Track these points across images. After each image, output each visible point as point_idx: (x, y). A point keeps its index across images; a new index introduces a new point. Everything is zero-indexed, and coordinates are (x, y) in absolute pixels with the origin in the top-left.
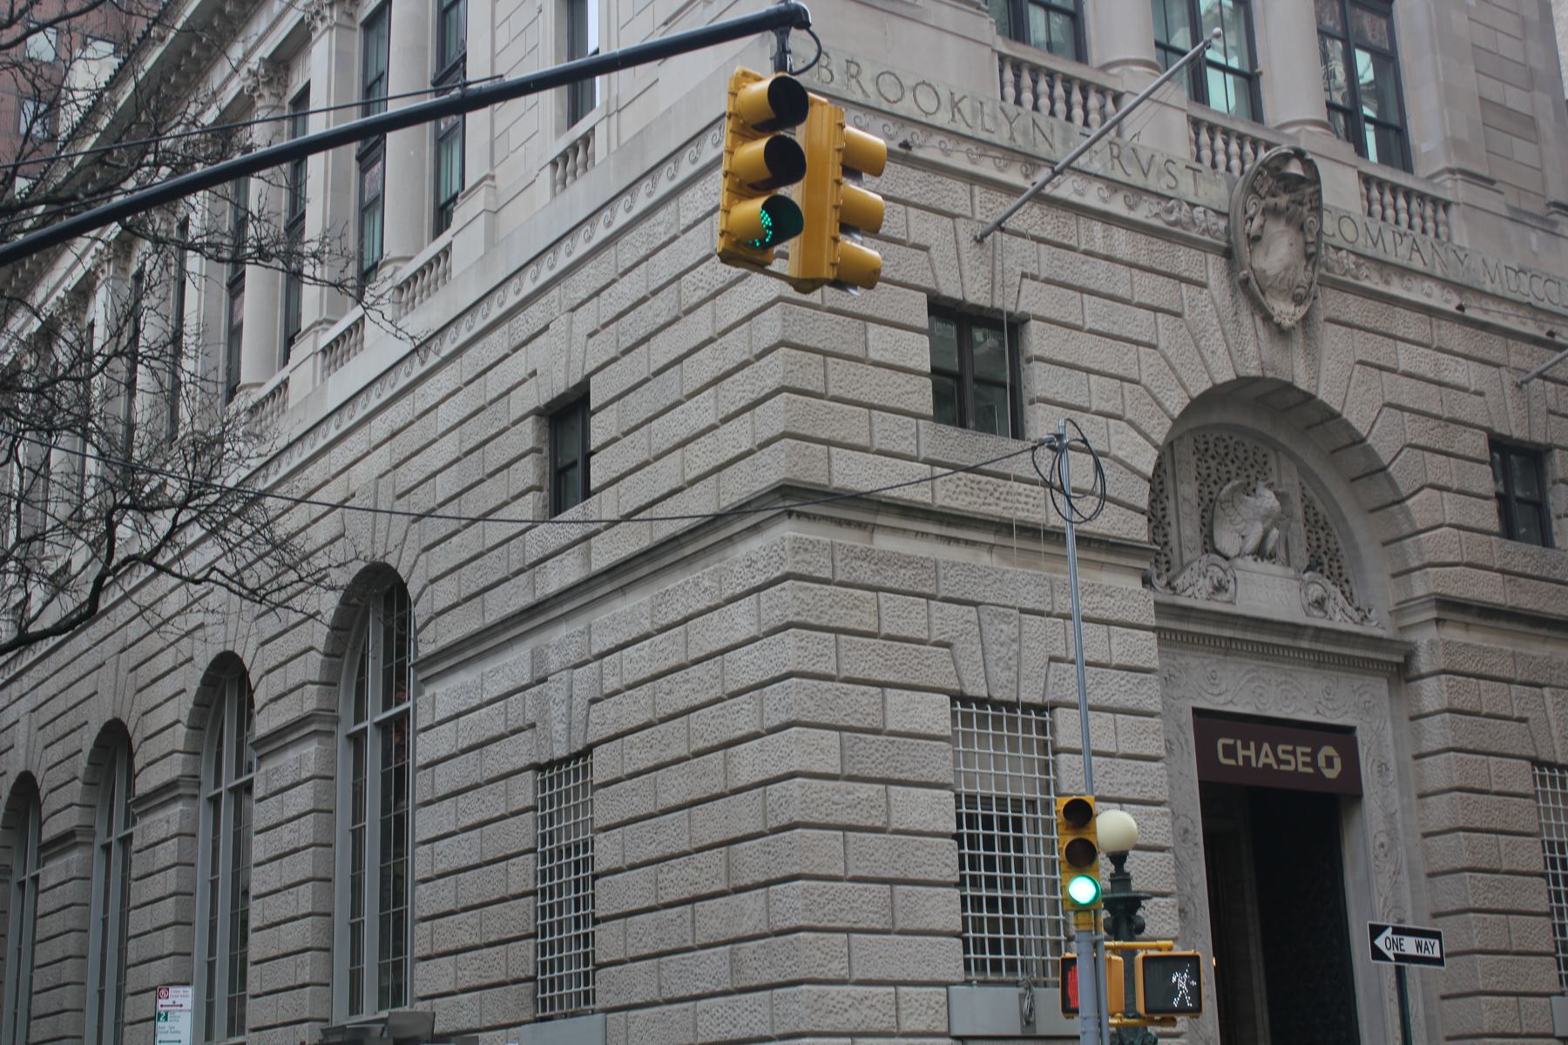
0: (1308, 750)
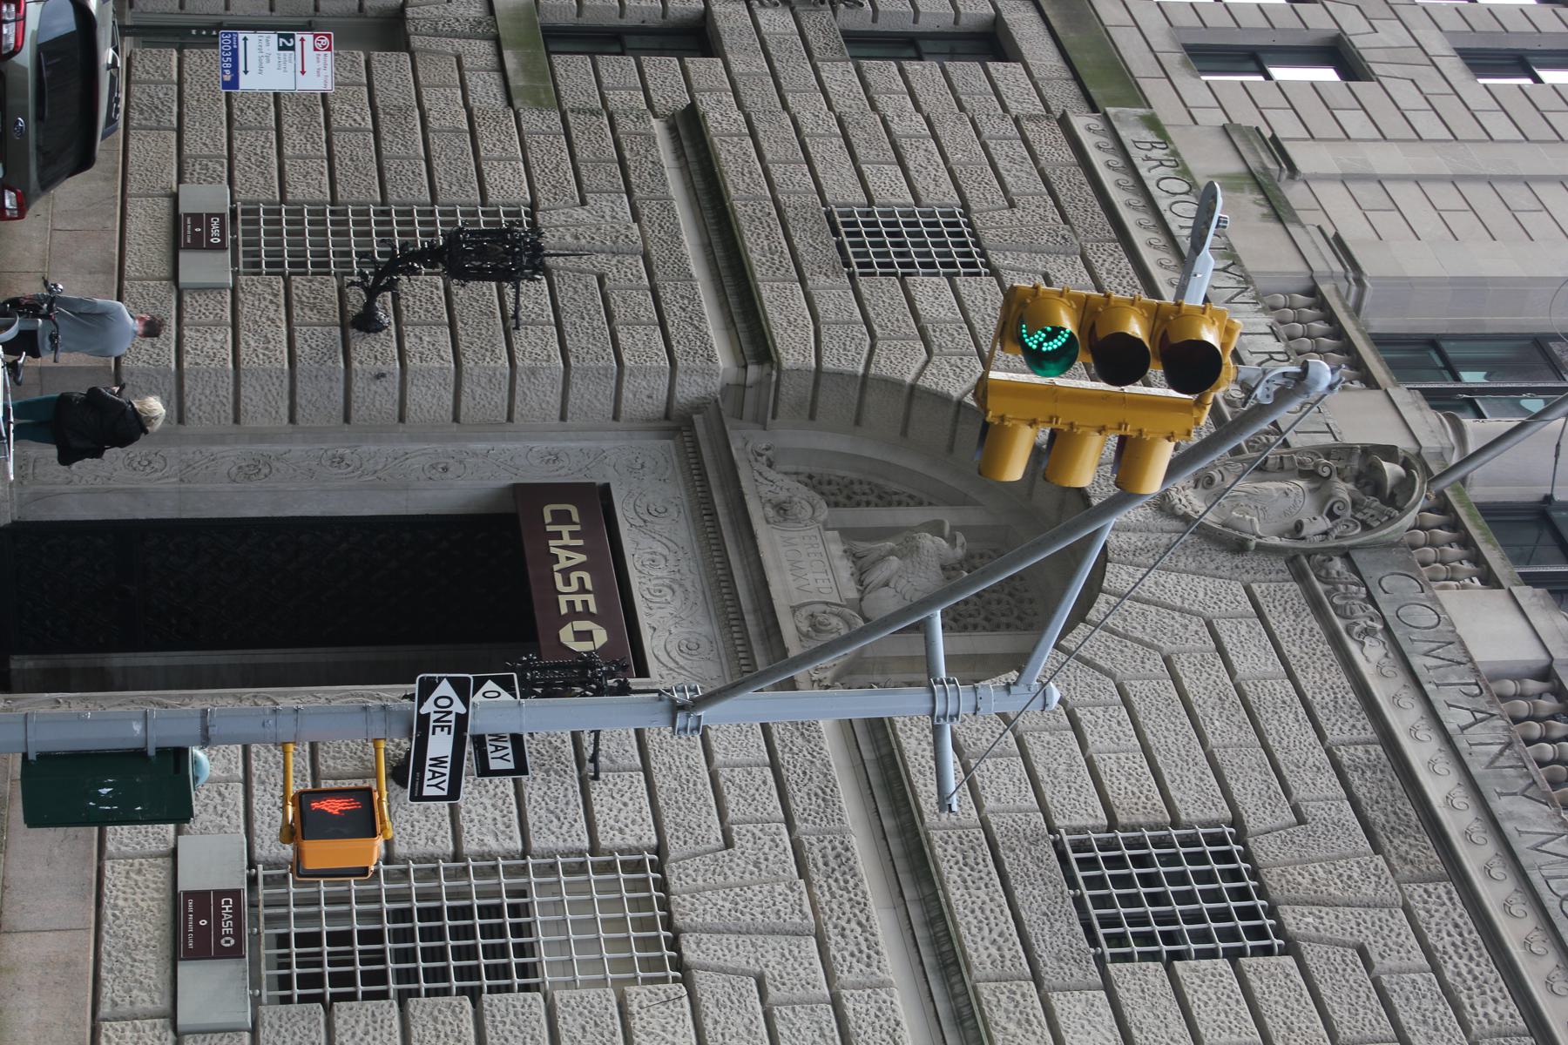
0: (593, 608)
